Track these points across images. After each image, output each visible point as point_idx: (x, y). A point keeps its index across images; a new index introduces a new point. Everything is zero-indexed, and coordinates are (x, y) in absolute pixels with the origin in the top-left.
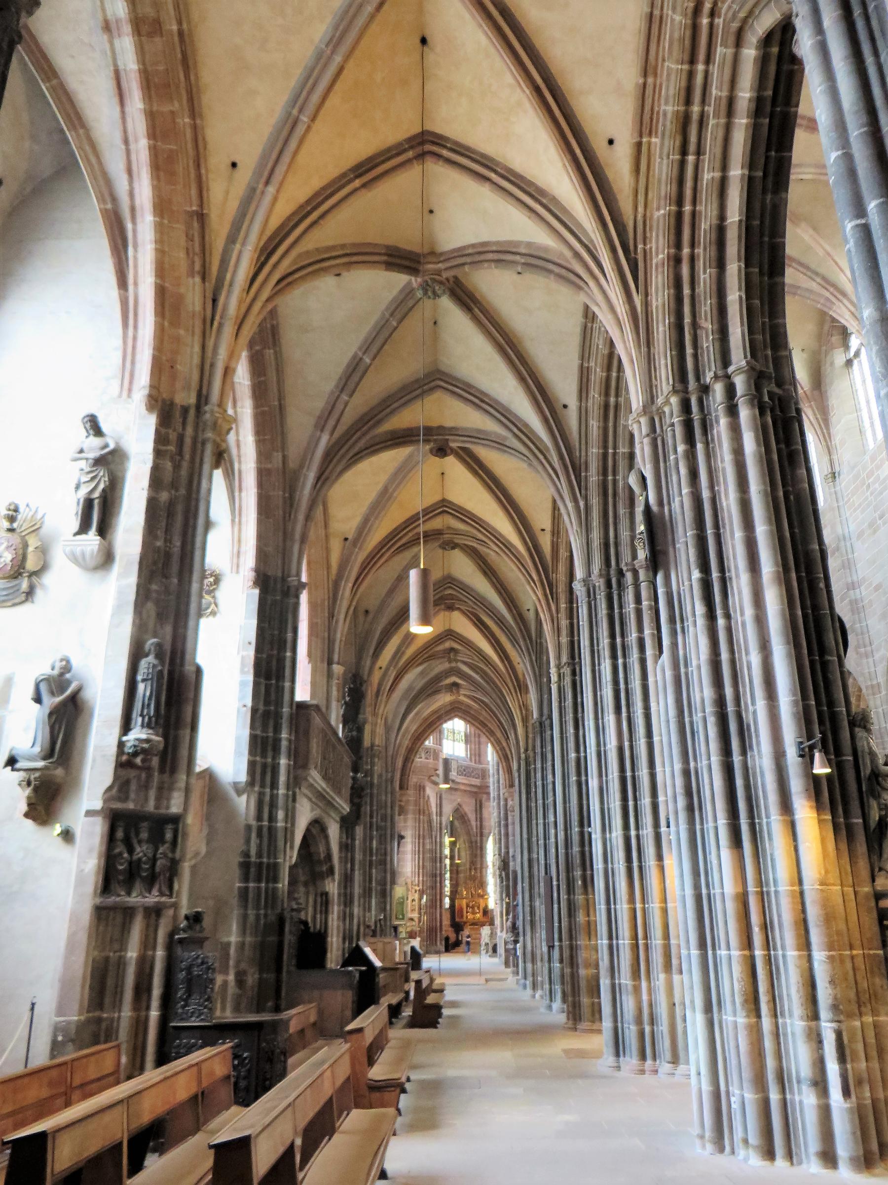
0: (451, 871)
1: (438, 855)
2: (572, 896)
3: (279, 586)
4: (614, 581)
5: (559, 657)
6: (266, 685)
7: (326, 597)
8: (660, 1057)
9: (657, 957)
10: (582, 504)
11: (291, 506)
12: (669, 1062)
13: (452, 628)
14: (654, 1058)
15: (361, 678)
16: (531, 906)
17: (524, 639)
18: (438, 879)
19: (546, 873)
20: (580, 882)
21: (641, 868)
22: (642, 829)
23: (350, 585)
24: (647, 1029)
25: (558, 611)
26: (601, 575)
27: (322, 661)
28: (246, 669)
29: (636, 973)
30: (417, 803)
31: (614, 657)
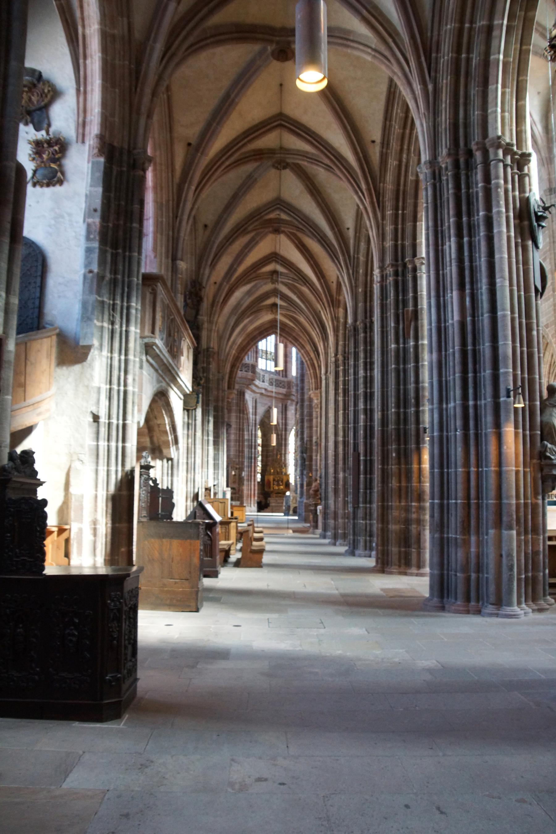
0: (262, 455)
1: (253, 444)
2: (386, 467)
3: (125, 158)
4: (462, 160)
5: (382, 260)
8: (483, 599)
9: (488, 515)
10: (430, 87)
11: (137, 78)
12: (493, 604)
13: (278, 251)
14: (478, 600)
15: (200, 284)
16: (335, 477)
17: (343, 255)
18: (253, 461)
19: (354, 450)
20: (394, 455)
21: (477, 435)
22: (480, 400)
24: (473, 576)
25: (383, 218)
26: (449, 155)
27: (167, 257)
28: (92, 236)
29: (466, 529)
30: (238, 405)
31: (459, 236)
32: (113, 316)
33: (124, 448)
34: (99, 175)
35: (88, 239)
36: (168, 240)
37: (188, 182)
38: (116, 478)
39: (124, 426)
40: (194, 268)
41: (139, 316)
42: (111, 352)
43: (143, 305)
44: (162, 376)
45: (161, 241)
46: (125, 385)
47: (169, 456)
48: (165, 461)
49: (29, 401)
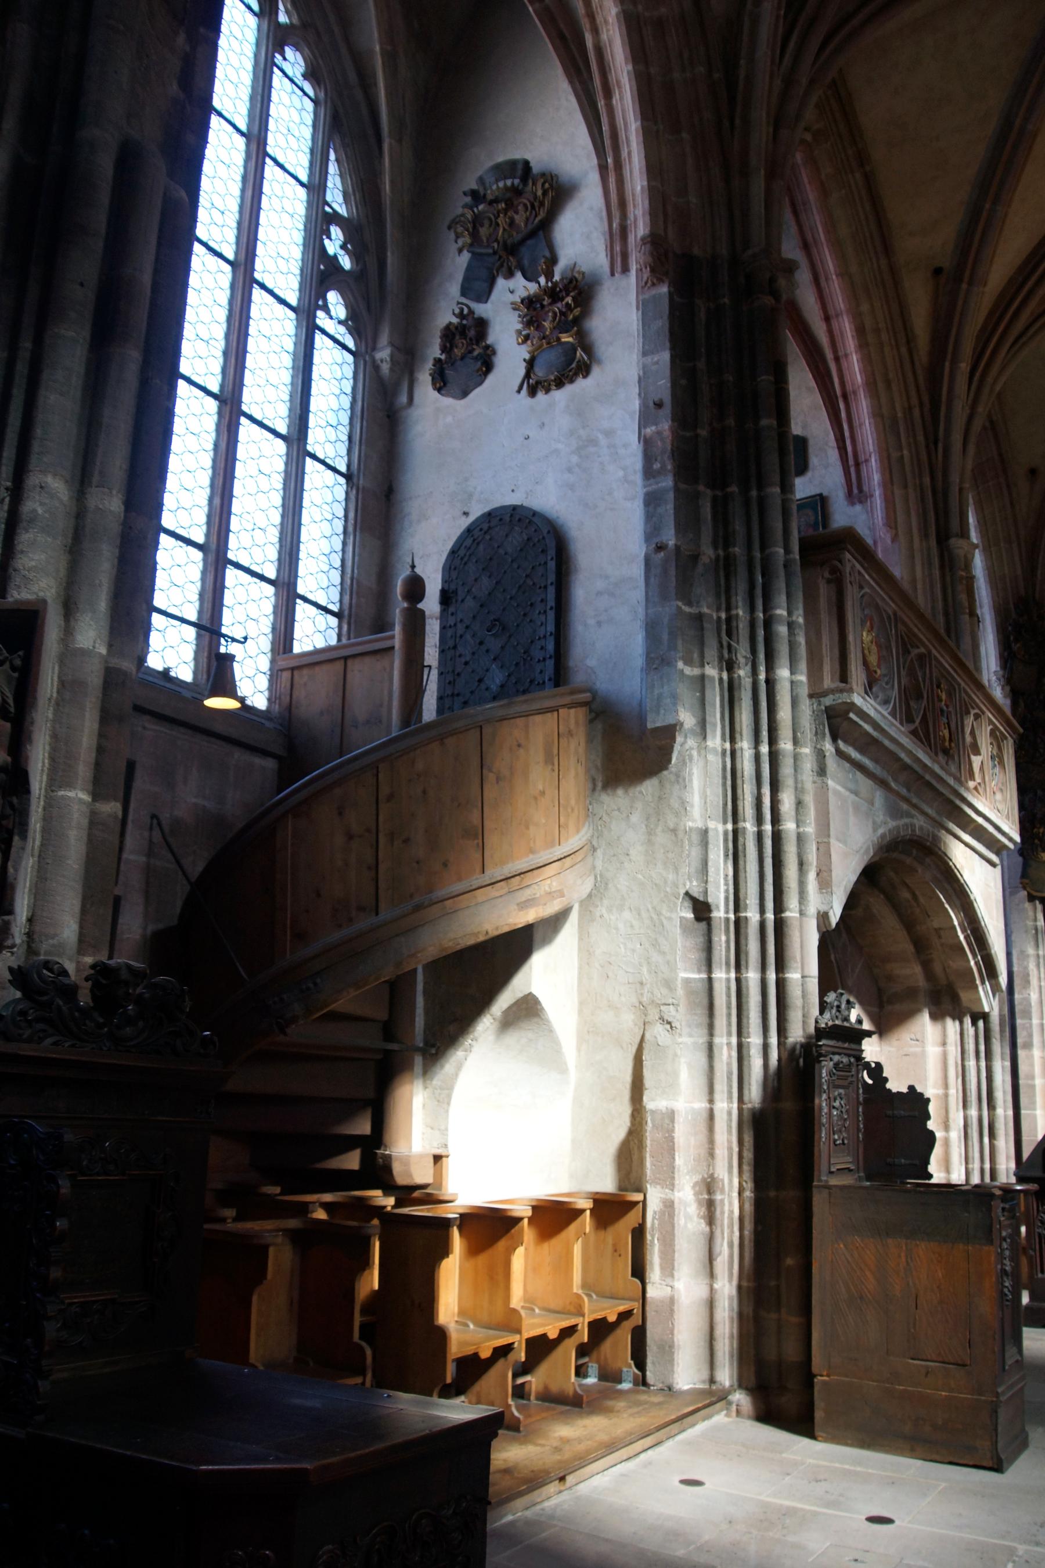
6: (715, 500)
7: (915, 401)
23: (964, 366)
27: (925, 536)
28: (657, 466)
32: (729, 646)
33: (781, 984)
34: (661, 324)
35: (649, 473)
36: (923, 498)
37: (949, 357)
38: (766, 1065)
39: (780, 925)
40: (1019, 572)
41: (801, 639)
42: (733, 740)
43: (811, 613)
44: (907, 800)
45: (906, 500)
46: (776, 820)
47: (976, 1009)
48: (968, 1021)
49: (495, 872)
